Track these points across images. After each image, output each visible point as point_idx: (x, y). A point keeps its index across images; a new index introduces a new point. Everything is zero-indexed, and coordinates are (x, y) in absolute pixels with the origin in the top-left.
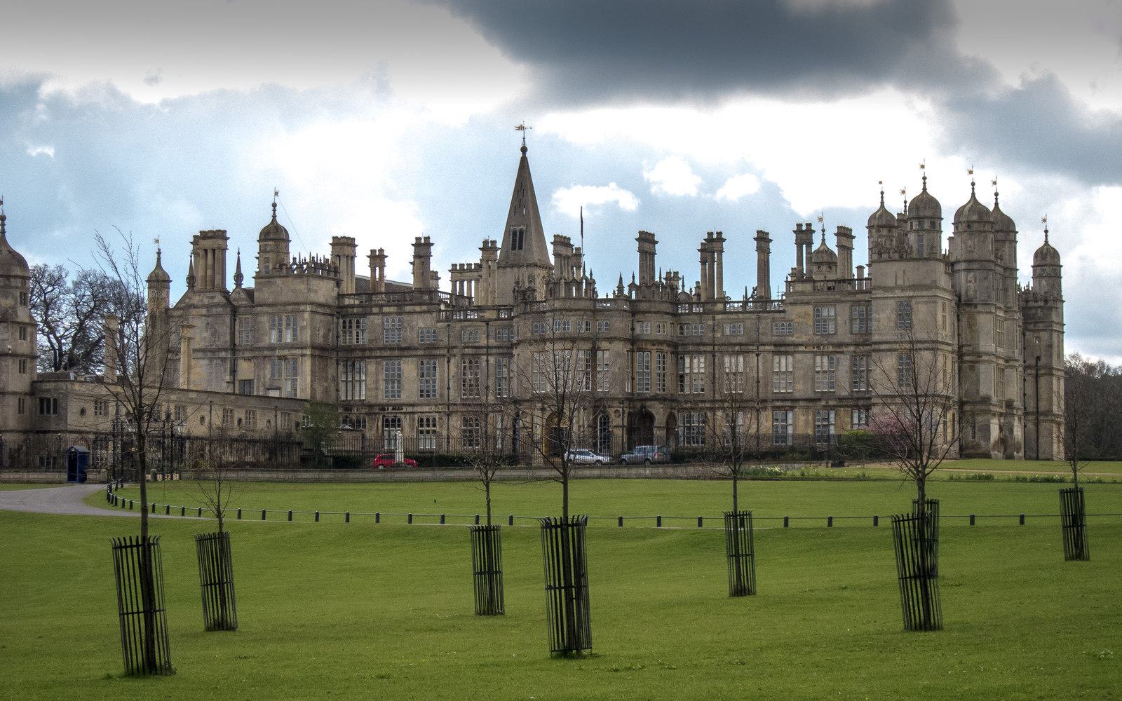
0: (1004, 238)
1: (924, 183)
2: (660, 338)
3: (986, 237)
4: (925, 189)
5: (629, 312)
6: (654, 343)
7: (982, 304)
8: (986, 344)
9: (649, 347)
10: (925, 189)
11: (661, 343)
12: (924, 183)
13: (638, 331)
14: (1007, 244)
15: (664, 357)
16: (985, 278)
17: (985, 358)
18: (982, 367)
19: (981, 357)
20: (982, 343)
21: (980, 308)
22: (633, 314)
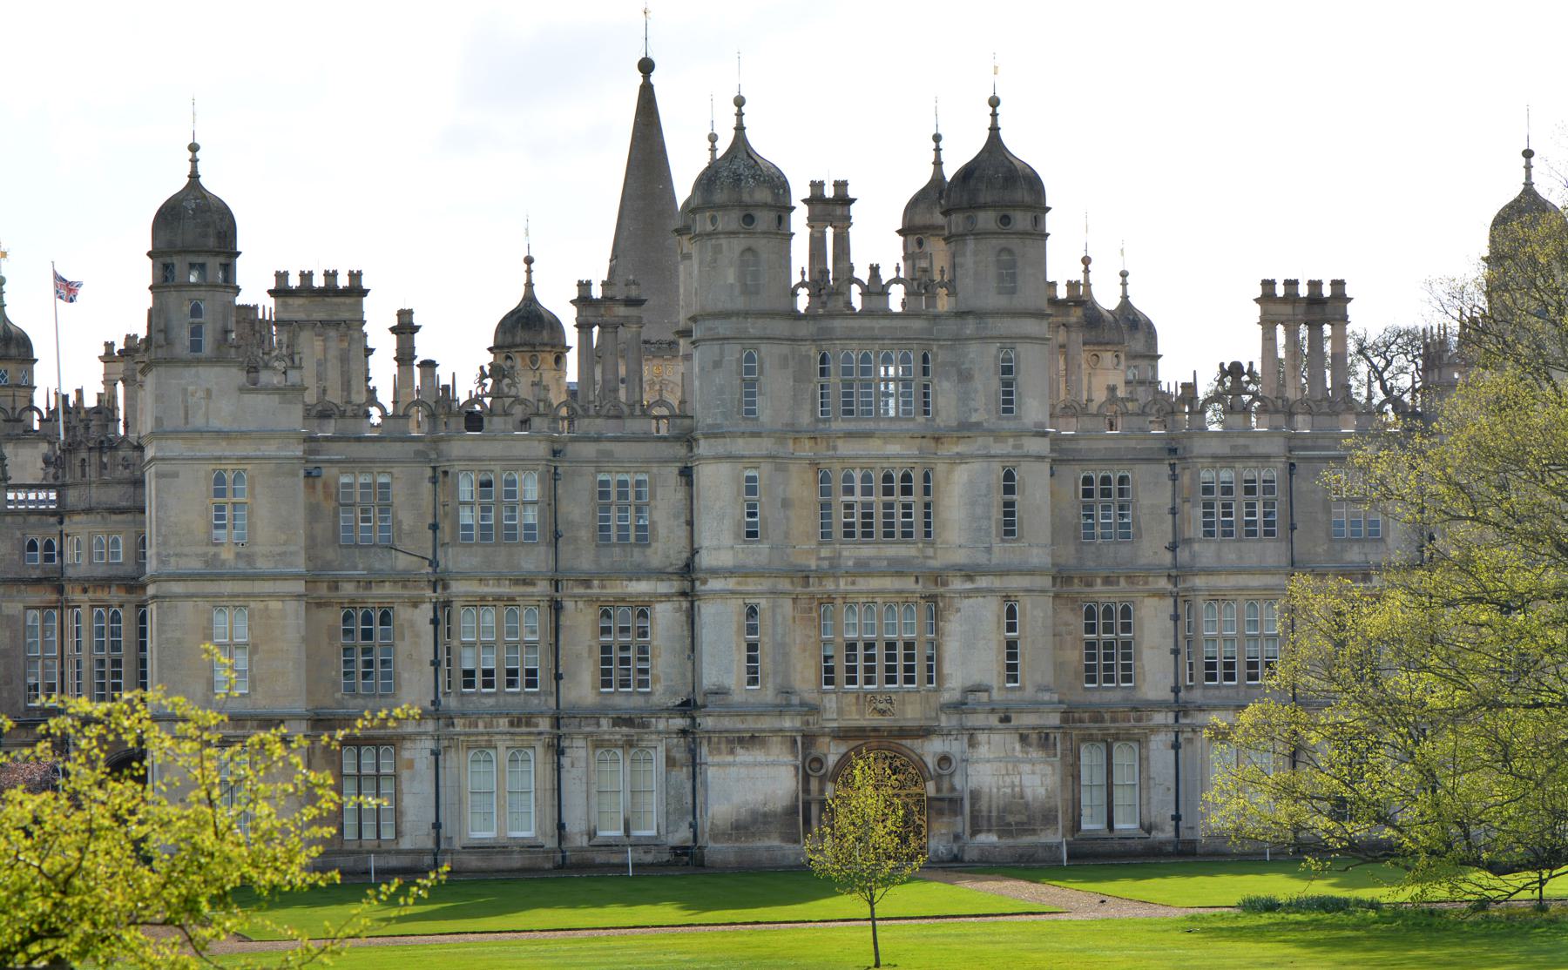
0: (961, 229)
1: (194, 161)
2: (100, 572)
3: (717, 250)
4: (194, 176)
5: (53, 513)
6: (87, 584)
7: (707, 436)
8: (719, 545)
9: (76, 595)
10: (194, 176)
11: (105, 582)
12: (194, 161)
13: (67, 560)
14: (971, 244)
15: (116, 618)
16: (717, 364)
17: (715, 584)
18: (708, 611)
19: (704, 582)
20: (705, 543)
21: (703, 447)
22: (61, 514)
